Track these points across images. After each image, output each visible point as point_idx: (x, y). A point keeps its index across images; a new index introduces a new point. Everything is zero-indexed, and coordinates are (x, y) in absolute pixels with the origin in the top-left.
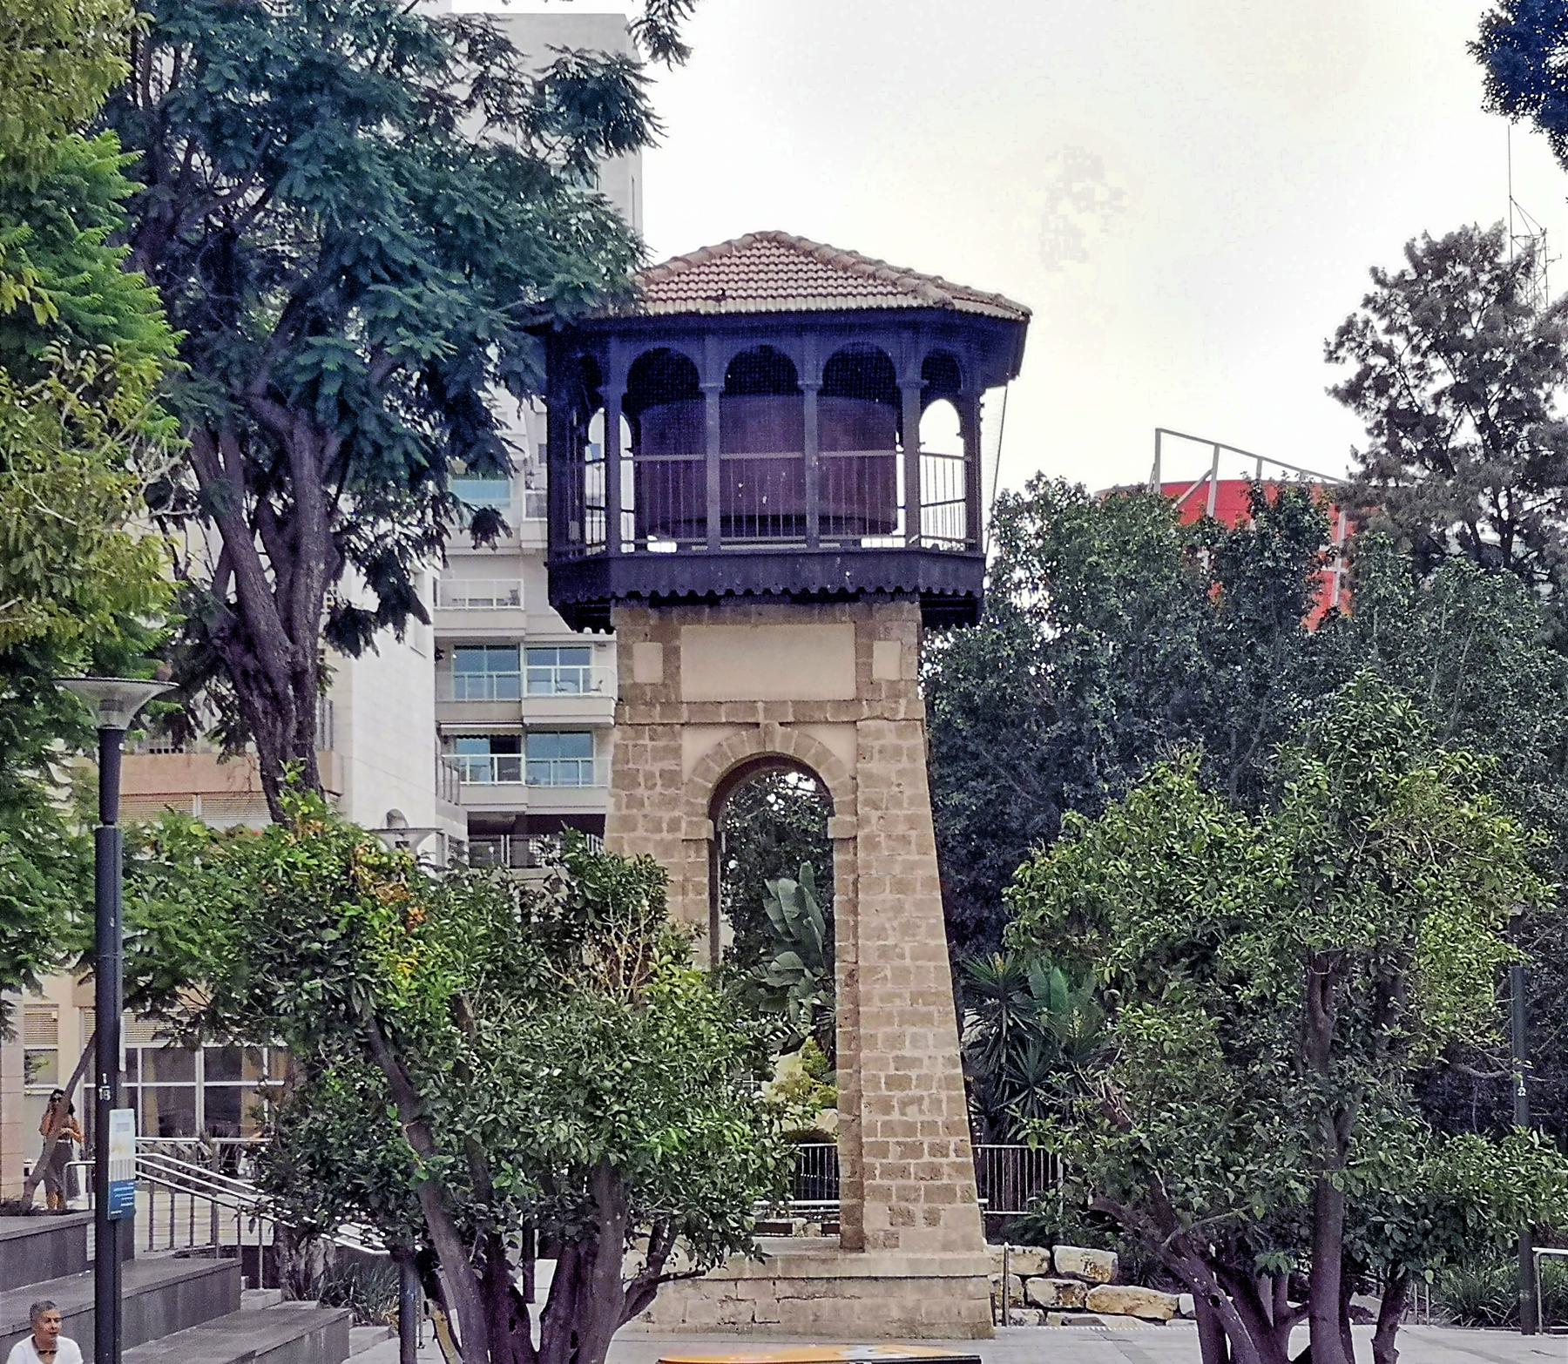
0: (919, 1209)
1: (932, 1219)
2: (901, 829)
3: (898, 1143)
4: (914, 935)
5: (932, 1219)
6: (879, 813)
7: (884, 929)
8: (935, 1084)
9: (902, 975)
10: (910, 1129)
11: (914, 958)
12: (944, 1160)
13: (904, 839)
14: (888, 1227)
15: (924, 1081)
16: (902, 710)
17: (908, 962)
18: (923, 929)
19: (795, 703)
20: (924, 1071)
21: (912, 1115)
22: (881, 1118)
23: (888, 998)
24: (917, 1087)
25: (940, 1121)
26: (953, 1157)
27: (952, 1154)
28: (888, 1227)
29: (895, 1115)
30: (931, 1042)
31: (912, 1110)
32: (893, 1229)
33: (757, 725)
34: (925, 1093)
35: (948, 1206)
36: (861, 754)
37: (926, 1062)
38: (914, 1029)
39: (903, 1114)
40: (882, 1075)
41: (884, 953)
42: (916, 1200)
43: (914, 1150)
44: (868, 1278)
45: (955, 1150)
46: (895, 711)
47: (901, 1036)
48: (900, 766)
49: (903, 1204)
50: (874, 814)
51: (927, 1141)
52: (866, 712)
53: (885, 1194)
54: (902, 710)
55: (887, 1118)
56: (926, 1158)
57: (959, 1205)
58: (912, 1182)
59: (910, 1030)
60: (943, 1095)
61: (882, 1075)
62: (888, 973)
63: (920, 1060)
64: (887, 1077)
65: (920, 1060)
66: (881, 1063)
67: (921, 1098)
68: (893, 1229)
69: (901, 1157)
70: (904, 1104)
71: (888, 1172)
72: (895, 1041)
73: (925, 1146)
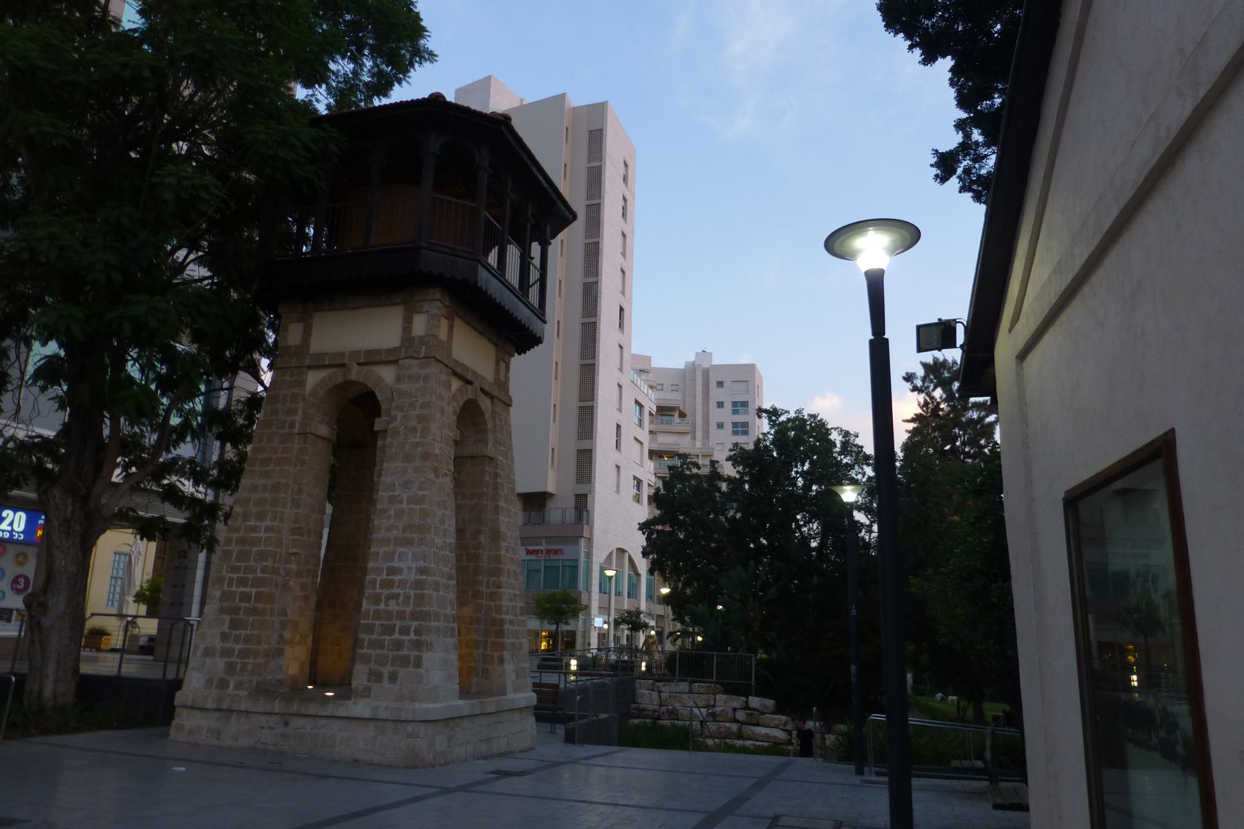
0: (386, 671)
1: (393, 678)
2: (413, 423)
5: (393, 678)
9: (400, 513)
10: (389, 615)
11: (408, 503)
13: (414, 430)
14: (365, 682)
15: (402, 584)
17: (404, 505)
18: (416, 485)
19: (366, 352)
20: (403, 577)
21: (393, 606)
22: (372, 608)
23: (389, 529)
25: (408, 610)
26: (412, 636)
27: (412, 633)
29: (382, 606)
31: (392, 603)
33: (344, 365)
34: (402, 592)
36: (398, 379)
37: (405, 571)
41: (392, 500)
43: (389, 630)
46: (419, 352)
47: (394, 553)
50: (400, 415)
51: (398, 624)
52: (403, 355)
56: (396, 636)
57: (412, 670)
58: (385, 652)
59: (400, 549)
60: (412, 593)
62: (392, 512)
64: (382, 581)
66: (379, 571)
70: (388, 598)
71: (373, 644)
72: (390, 556)
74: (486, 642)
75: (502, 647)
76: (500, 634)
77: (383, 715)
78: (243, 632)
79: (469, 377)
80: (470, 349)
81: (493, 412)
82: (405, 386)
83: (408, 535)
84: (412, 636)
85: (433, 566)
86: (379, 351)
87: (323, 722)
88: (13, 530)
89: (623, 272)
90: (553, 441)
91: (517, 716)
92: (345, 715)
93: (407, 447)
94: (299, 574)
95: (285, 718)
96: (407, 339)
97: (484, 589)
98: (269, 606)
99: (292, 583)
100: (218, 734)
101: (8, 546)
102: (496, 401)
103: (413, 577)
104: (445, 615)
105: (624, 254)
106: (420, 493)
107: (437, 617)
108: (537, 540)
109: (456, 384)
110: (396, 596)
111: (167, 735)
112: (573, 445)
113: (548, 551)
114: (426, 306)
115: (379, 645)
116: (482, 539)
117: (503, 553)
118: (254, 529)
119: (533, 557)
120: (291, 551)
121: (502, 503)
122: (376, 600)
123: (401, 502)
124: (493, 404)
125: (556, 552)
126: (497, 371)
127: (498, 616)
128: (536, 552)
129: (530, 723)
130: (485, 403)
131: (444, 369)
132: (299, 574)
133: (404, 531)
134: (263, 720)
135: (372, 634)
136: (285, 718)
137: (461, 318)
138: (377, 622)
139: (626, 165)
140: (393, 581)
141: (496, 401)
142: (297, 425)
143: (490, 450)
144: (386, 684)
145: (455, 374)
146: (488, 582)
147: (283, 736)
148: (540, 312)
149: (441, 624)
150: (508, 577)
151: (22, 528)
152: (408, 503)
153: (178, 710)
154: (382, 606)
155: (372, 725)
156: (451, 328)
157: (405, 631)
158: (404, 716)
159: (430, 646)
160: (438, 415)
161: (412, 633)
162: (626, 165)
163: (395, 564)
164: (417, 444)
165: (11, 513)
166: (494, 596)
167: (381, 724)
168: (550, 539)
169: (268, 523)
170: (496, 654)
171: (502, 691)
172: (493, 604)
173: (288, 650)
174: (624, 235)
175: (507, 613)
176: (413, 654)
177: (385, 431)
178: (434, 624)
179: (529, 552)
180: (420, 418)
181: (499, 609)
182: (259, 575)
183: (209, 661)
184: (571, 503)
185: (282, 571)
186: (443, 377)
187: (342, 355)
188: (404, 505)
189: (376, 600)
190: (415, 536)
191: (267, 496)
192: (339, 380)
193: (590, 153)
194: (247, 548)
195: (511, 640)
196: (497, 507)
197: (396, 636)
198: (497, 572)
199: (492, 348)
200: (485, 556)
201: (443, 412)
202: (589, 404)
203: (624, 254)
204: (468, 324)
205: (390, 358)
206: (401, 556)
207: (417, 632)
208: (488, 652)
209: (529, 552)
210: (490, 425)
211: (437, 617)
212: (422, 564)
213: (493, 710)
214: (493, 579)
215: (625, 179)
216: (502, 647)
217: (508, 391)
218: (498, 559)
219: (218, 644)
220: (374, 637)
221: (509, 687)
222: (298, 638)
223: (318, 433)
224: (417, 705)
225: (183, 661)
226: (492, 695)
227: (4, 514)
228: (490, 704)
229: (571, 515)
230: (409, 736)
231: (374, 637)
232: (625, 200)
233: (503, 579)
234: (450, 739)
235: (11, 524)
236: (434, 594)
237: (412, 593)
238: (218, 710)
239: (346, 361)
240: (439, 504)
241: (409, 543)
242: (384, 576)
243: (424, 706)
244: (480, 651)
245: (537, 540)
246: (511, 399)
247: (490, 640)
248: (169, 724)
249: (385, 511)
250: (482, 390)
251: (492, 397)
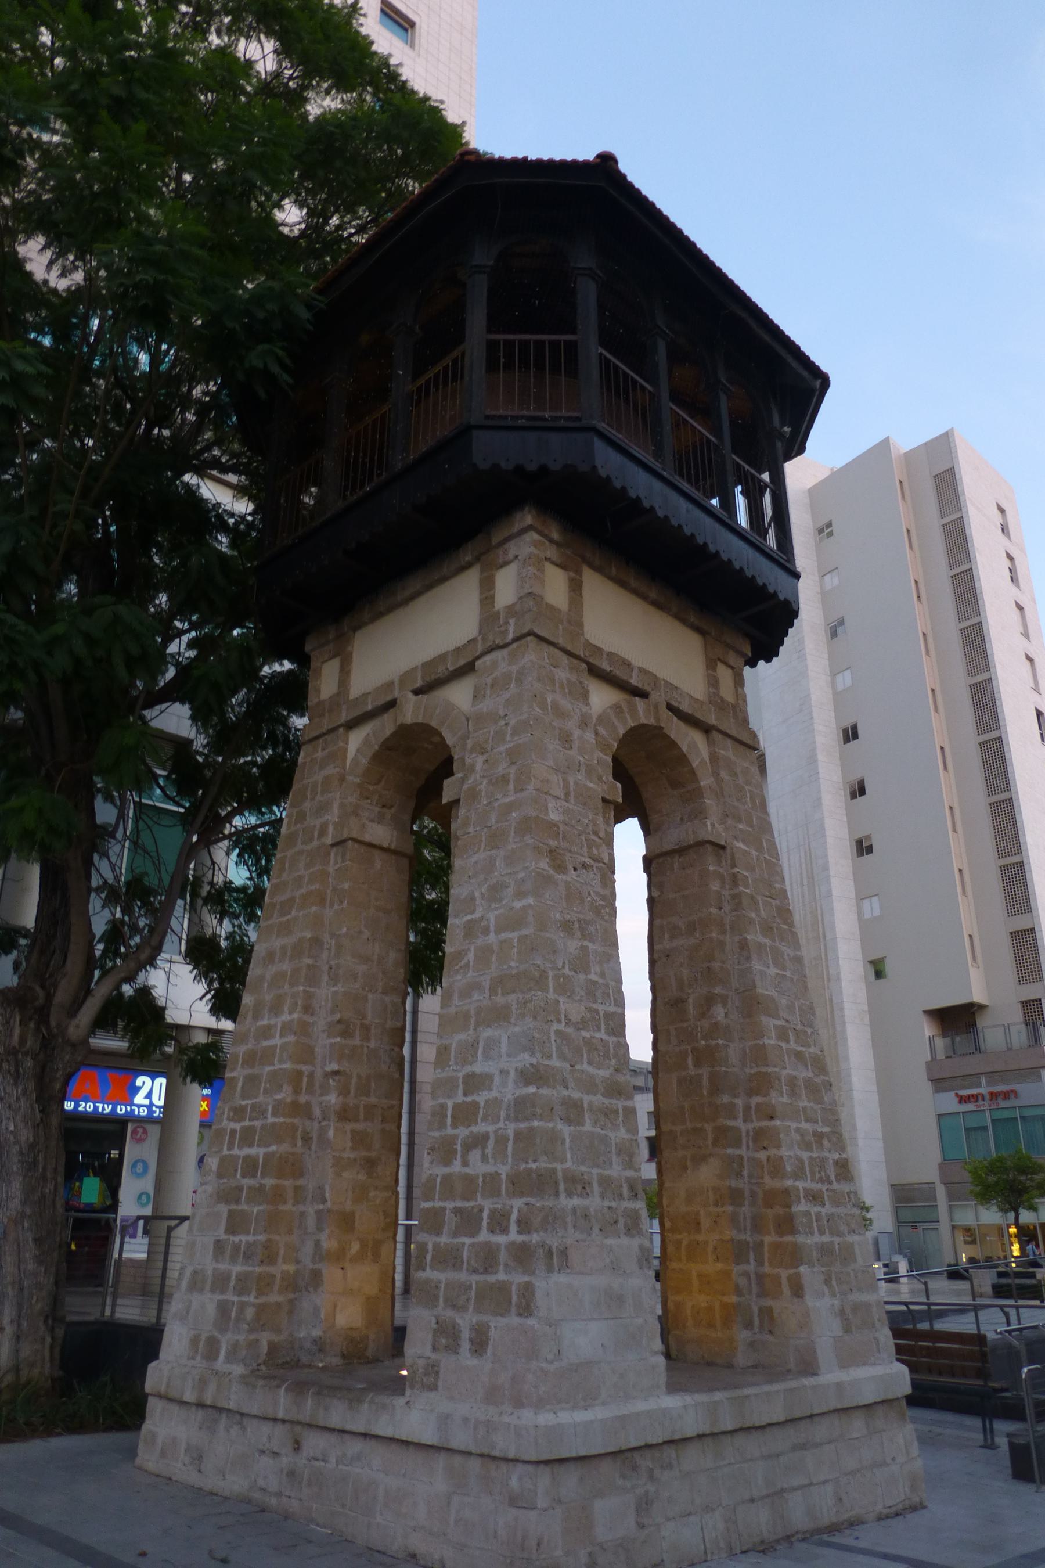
0: (465, 1321)
1: (479, 1345)
2: (501, 769)
3: (457, 1211)
4: (501, 900)
6: (485, 757)
7: (473, 898)
8: (503, 1114)
11: (498, 932)
12: (501, 1239)
13: (505, 779)
14: (428, 1353)
16: (511, 629)
18: (510, 891)
20: (494, 1094)
21: (477, 1166)
22: (440, 1171)
24: (485, 1119)
25: (504, 1170)
26: (514, 1236)
27: (513, 1228)
28: (428, 1353)
29: (457, 1167)
30: (504, 1049)
31: (475, 1155)
32: (434, 1356)
34: (490, 1129)
35: (502, 1321)
37: (497, 1080)
39: (465, 1164)
40: (450, 1104)
42: (463, 1309)
43: (469, 1222)
44: (392, 1440)
45: (519, 1222)
48: (507, 695)
49: (450, 1313)
51: (488, 1205)
52: (480, 648)
54: (511, 629)
55: (447, 1170)
56: (484, 1236)
57: (514, 1320)
58: (462, 1276)
59: (487, 1033)
61: (450, 1104)
62: (471, 956)
63: (490, 1077)
64: (456, 1106)
65: (490, 1077)
67: (485, 1137)
68: (434, 1356)
73: (485, 1214)
74: (761, 1244)
75: (795, 1256)
76: (787, 1224)
77: (460, 1439)
78: (244, 1238)
79: (634, 681)
80: (623, 625)
81: (714, 758)
82: (486, 706)
83: (499, 999)
84: (514, 1236)
85: (555, 1063)
86: (442, 658)
87: (356, 1446)
88: (152, 1104)
89: (1030, 659)
90: (968, 924)
91: (858, 1425)
92: (388, 1432)
93: (494, 816)
94: (344, 1115)
95: (298, 1429)
96: (489, 617)
97: (739, 1123)
98: (288, 1183)
99: (331, 1133)
100: (198, 1458)
101: (149, 1127)
102: (714, 733)
103: (508, 1091)
104: (606, 1183)
105: (1026, 635)
106: (518, 905)
107: (577, 1184)
108: (973, 1079)
109: (601, 698)
110: (479, 1141)
111: (132, 1453)
112: (1002, 925)
113: (993, 1096)
114: (512, 548)
115: (449, 1258)
116: (719, 1012)
117: (771, 1041)
118: (266, 1032)
119: (970, 1107)
120: (328, 1069)
121: (754, 936)
122: (445, 1152)
123: (486, 931)
124: (710, 743)
125: (1006, 1095)
126: (713, 682)
127: (777, 1184)
128: (973, 1098)
129: (901, 1441)
130: (692, 743)
131: (564, 659)
132: (344, 1115)
133: (493, 991)
134: (263, 1434)
135: (439, 1234)
136: (298, 1429)
137: (592, 566)
138: (449, 1205)
139: (1002, 510)
140: (475, 1105)
141: (714, 733)
142: (331, 828)
143: (713, 828)
144: (466, 1358)
145: (595, 672)
146: (747, 1108)
147: (292, 1474)
148: (784, 559)
149: (594, 1203)
150: (793, 1093)
151: (161, 1103)
152: (498, 932)
153: (152, 1402)
154: (457, 1167)
155: (441, 1461)
156: (576, 587)
157: (499, 1222)
158: (503, 1444)
159: (559, 1259)
160: (553, 745)
161: (513, 1228)
162: (1002, 510)
163: (478, 1068)
164: (510, 807)
165: (147, 1079)
166: (762, 1138)
167: (457, 1460)
168: (992, 1076)
169: (286, 1017)
170: (784, 1274)
171: (809, 1367)
172: (762, 1155)
173: (331, 1273)
174: (1020, 608)
175: (799, 1173)
176: (518, 1278)
177: (458, 801)
178: (566, 1202)
179: (962, 1100)
180: (513, 755)
181: (776, 1168)
182: (271, 1120)
183: (196, 1299)
184: (1017, 1016)
185: (317, 1112)
186: (562, 674)
187: (389, 685)
188: (492, 937)
189: (445, 1152)
190: (512, 998)
191: (286, 966)
192: (388, 732)
193: (941, 505)
194: (255, 1071)
195: (817, 1238)
196: (744, 945)
197: (484, 1236)
198: (761, 1084)
199: (694, 640)
200: (733, 1052)
201: (566, 740)
202: (1015, 859)
203: (1026, 635)
204: (622, 584)
206: (491, 1044)
207: (524, 1226)
208: (767, 1269)
209: (962, 1100)
210: (706, 781)
211: (577, 1184)
212: (526, 1059)
213: (778, 1414)
214: (755, 1100)
215: (1004, 529)
216: (795, 1256)
217: (745, 721)
218: (760, 1055)
219: (209, 1265)
220: (444, 1239)
221: (825, 1352)
222: (355, 1247)
223: (367, 838)
224: (527, 1417)
225: (162, 1297)
226: (786, 1374)
227: (139, 1082)
228: (767, 1400)
229: (1019, 1035)
230: (514, 1501)
231: (444, 1239)
232: (1010, 558)
233: (779, 1099)
234: (644, 1505)
235: (149, 1096)
236: (566, 1131)
237: (511, 1129)
238: (200, 1405)
239: (396, 694)
240: (567, 927)
241: (500, 1016)
242: (460, 1098)
243: (546, 1419)
244: (751, 1267)
245: (973, 1079)
246: (754, 735)
247: (768, 1239)
248: (138, 1428)
249: (460, 955)
250: (670, 708)
251: (706, 729)
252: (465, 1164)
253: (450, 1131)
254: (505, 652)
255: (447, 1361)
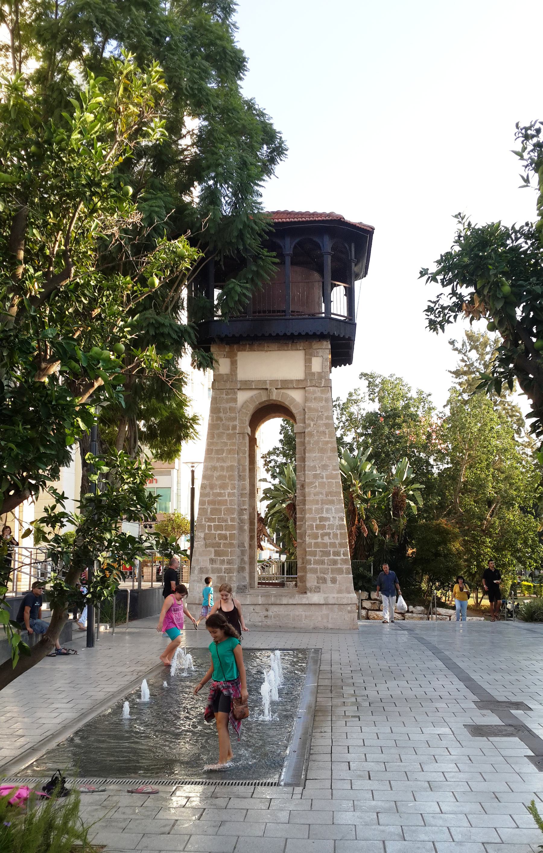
0: (328, 577)
1: (334, 581)
2: (322, 429)
3: (321, 551)
5: (334, 581)
7: (315, 467)
9: (322, 485)
10: (325, 545)
13: (324, 433)
14: (316, 584)
15: (331, 527)
16: (323, 383)
17: (325, 480)
18: (331, 468)
20: (331, 522)
21: (326, 540)
22: (313, 541)
25: (337, 542)
26: (342, 556)
27: (342, 556)
29: (319, 540)
33: (267, 389)
37: (332, 519)
38: (327, 506)
40: (314, 524)
41: (316, 476)
43: (327, 554)
46: (321, 383)
49: (322, 575)
51: (332, 550)
52: (309, 384)
53: (315, 571)
56: (332, 557)
58: (326, 566)
60: (338, 532)
61: (314, 524)
65: (329, 518)
66: (314, 519)
67: (330, 533)
69: (321, 556)
70: (323, 535)
86: (291, 381)
92: (307, 603)
95: (266, 606)
110: (329, 534)
114: (321, 352)
122: (316, 537)
135: (315, 556)
140: (325, 525)
154: (319, 540)
155: (324, 607)
163: (324, 515)
167: (330, 606)
188: (325, 480)
189: (316, 537)
192: (264, 399)
197: (332, 557)
205: (299, 385)
239: (268, 387)
252: (323, 540)
253: (315, 531)
254: (319, 389)
255: (322, 586)
